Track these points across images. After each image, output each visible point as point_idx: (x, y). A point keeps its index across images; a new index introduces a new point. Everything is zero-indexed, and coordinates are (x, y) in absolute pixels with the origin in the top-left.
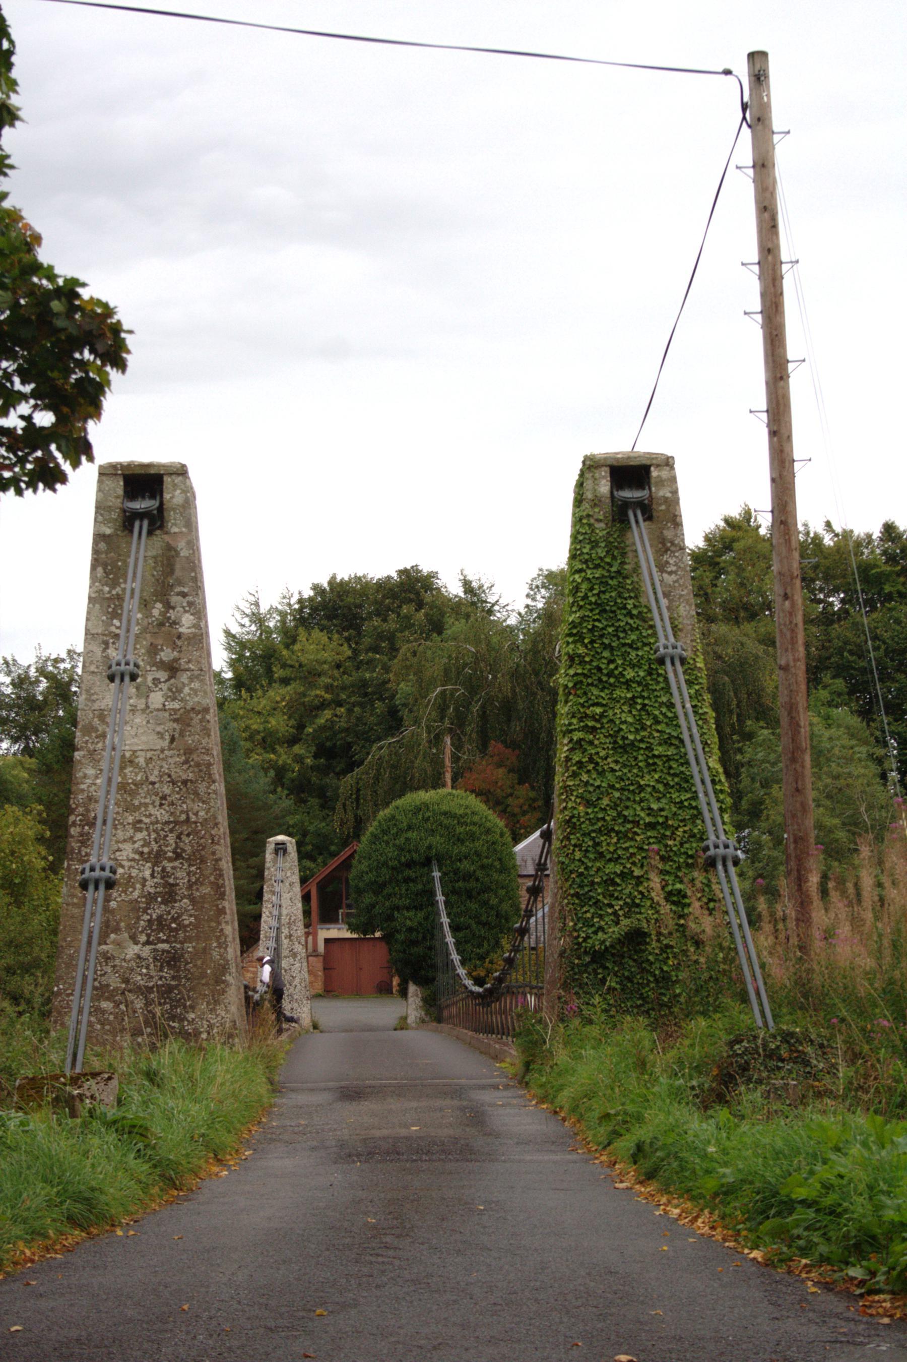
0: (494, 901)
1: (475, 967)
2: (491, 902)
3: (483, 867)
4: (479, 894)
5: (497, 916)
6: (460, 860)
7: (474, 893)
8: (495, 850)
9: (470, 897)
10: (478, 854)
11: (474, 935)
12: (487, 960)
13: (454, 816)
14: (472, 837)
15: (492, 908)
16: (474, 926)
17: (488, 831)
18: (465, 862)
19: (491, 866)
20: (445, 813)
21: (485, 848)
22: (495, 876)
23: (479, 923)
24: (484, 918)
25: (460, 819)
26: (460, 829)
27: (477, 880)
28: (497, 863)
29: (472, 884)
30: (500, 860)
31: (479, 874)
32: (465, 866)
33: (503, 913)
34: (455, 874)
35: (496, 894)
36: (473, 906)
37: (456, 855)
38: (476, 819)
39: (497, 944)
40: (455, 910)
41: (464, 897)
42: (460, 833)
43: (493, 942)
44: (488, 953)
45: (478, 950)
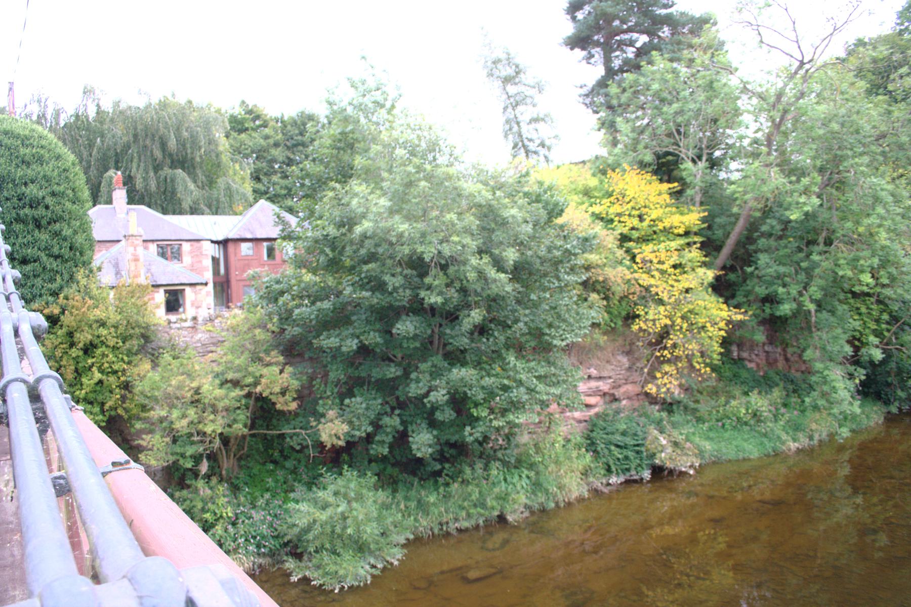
0: (67, 232)
1: (47, 303)
2: (64, 233)
3: (53, 194)
4: (49, 223)
5: (71, 249)
6: (26, 184)
7: (44, 222)
8: (67, 178)
9: (39, 226)
10: (47, 179)
11: (44, 268)
12: (61, 296)
13: (17, 137)
14: (40, 160)
15: (65, 239)
16: (45, 258)
17: (58, 157)
18: (31, 186)
19: (62, 194)
20: (6, 133)
21: (56, 173)
22: (68, 205)
23: (50, 256)
24: (56, 250)
25: (25, 141)
26: (23, 151)
27: (47, 207)
28: (69, 192)
29: (41, 211)
30: (73, 190)
31: (49, 200)
32: (32, 190)
33: (78, 245)
34: (20, 200)
35: (69, 225)
36: (43, 237)
37: (21, 178)
38: (43, 142)
39: (72, 277)
40: (20, 240)
41: (31, 227)
42: (25, 155)
43: (66, 277)
44: (61, 288)
45: (50, 285)
